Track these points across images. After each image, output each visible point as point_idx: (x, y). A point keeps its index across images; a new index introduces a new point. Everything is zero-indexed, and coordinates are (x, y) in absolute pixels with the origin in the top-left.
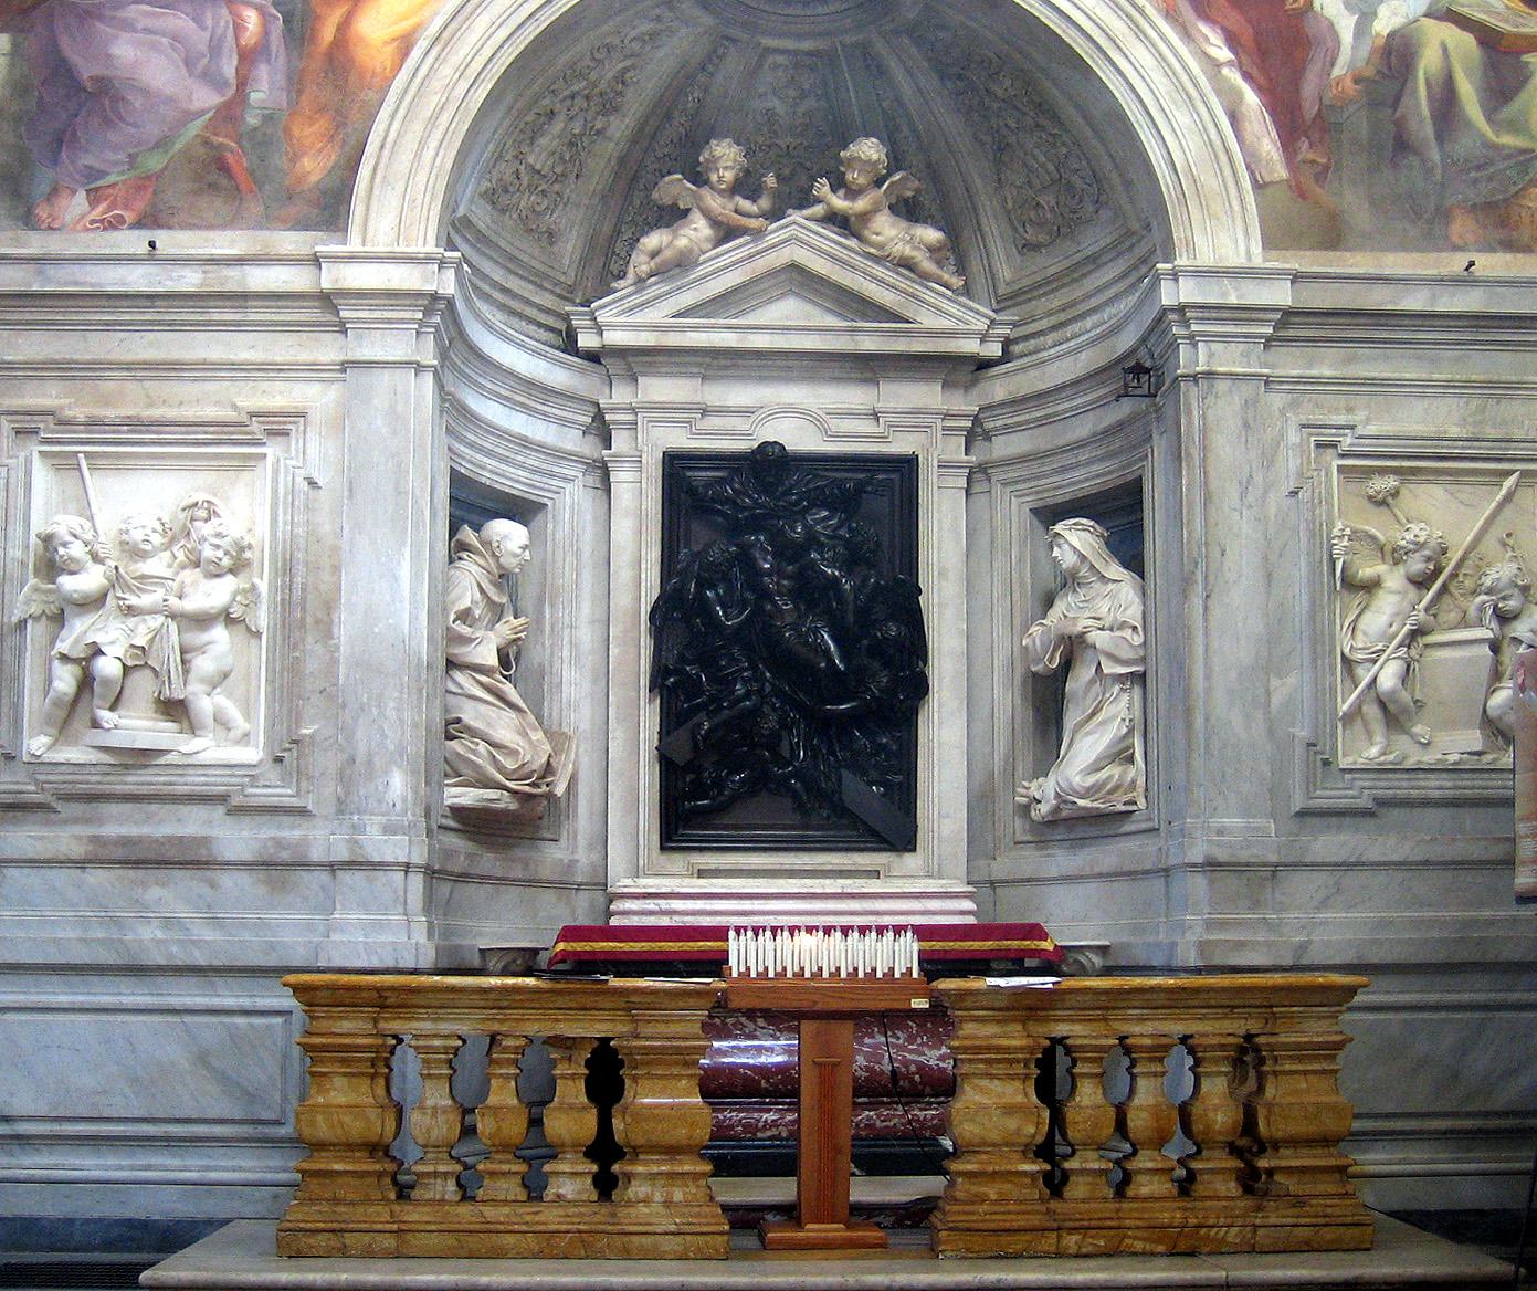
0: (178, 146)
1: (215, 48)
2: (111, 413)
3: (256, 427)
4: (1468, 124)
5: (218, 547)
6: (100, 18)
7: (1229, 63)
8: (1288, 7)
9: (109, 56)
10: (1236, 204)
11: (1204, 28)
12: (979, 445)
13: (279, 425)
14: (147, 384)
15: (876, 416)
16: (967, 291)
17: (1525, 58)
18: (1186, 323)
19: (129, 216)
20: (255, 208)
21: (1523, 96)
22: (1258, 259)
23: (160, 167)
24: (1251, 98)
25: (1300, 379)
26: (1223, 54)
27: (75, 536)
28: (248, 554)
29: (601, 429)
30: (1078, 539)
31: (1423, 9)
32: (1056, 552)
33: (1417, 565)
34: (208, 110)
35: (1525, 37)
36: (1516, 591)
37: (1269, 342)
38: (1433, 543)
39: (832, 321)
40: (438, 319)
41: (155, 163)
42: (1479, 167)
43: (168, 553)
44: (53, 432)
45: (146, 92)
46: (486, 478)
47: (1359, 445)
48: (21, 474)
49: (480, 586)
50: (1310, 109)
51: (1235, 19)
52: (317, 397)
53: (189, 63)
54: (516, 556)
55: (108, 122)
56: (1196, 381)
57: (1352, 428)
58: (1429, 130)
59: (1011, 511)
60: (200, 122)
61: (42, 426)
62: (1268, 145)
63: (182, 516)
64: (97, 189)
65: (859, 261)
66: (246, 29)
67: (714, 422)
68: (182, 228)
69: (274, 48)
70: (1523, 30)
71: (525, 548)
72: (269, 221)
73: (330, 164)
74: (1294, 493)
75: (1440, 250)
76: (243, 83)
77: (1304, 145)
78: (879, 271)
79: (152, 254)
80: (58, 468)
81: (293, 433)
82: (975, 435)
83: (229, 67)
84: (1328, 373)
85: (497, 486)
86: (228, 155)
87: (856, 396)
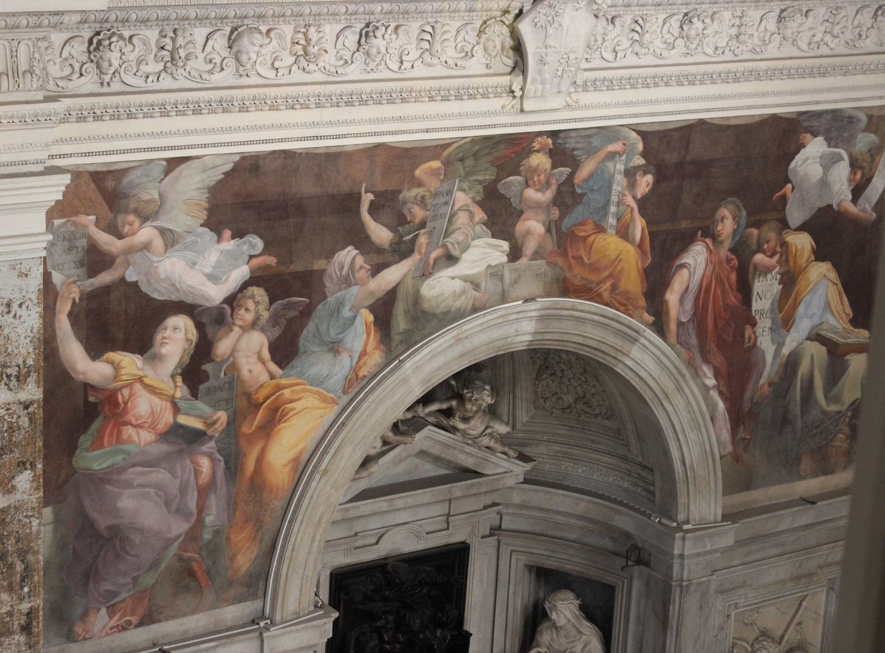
0: (164, 565)
4: (816, 402)
6: (109, 482)
8: (746, 346)
9: (117, 510)
11: (705, 368)
19: (135, 620)
20: (209, 596)
23: (153, 581)
26: (711, 382)
41: (149, 580)
42: (817, 427)
45: (142, 531)
50: (747, 406)
51: (719, 360)
53: (167, 504)
55: (118, 556)
60: (176, 545)
64: (113, 605)
66: (202, 472)
68: (167, 620)
69: (219, 485)
73: (253, 557)
75: (794, 481)
77: (741, 428)
86: (194, 564)
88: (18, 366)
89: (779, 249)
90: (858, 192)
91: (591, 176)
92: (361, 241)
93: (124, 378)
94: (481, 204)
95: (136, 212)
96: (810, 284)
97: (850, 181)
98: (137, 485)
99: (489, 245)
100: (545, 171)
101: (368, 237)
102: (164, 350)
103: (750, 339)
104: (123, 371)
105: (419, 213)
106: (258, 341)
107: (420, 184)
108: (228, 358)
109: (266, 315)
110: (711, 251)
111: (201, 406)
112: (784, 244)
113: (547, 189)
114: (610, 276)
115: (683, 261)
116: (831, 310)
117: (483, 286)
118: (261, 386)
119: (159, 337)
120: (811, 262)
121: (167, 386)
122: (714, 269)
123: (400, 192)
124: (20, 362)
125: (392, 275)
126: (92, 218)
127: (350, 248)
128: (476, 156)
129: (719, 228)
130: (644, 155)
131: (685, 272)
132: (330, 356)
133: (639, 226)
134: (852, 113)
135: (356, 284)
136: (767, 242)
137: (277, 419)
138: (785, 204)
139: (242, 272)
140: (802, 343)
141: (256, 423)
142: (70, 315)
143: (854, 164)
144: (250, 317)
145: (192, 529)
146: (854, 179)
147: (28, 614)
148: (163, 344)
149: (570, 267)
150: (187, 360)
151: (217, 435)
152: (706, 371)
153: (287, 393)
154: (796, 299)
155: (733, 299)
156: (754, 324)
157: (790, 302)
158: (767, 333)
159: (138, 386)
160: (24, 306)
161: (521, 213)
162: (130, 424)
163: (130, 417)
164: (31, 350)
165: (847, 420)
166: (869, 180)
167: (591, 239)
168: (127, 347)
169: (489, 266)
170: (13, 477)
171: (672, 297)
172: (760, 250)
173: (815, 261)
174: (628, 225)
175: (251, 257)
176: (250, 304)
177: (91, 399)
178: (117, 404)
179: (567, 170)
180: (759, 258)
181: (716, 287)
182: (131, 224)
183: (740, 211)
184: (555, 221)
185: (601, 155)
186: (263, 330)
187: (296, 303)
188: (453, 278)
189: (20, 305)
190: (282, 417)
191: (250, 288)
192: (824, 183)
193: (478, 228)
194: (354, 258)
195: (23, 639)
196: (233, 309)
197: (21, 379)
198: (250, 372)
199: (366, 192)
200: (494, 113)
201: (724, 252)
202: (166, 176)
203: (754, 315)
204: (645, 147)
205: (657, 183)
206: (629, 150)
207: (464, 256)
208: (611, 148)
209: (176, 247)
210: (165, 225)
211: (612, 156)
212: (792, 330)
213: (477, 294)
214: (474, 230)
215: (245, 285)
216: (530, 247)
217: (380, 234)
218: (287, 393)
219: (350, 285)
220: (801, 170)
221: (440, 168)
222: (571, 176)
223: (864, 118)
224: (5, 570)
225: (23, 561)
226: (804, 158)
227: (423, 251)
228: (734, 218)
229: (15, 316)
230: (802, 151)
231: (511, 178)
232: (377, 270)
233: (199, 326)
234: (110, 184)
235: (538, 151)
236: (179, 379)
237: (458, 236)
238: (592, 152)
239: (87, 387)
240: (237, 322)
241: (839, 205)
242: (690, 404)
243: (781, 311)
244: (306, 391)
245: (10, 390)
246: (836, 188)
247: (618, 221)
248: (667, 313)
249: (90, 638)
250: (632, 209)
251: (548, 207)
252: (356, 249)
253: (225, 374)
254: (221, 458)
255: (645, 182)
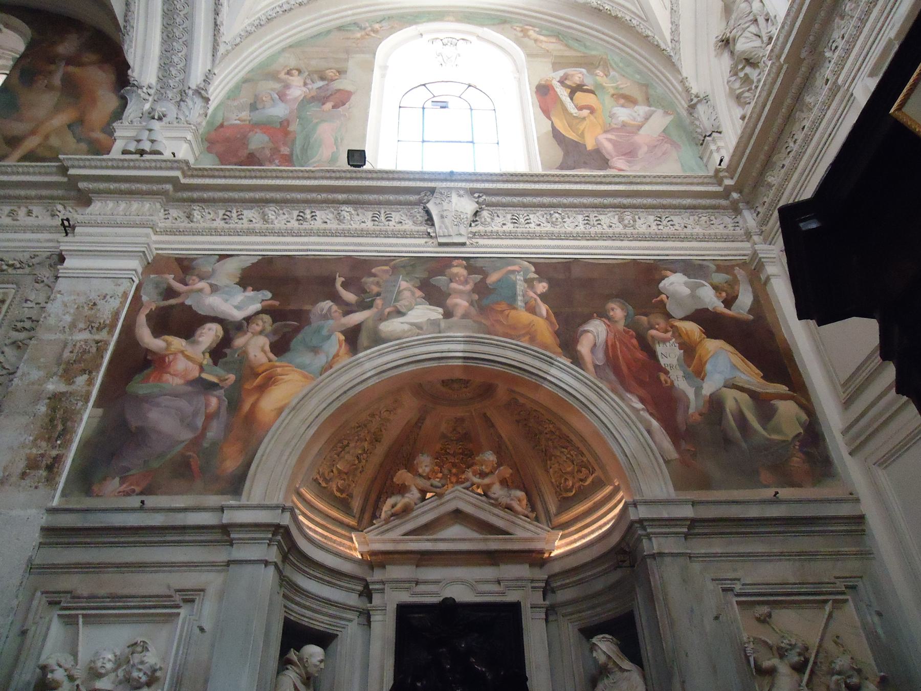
1: (195, 414)
2: (102, 592)
3: (178, 598)
4: (756, 431)
5: (140, 670)
7: (643, 409)
10: (658, 471)
12: (550, 595)
13: (190, 597)
14: (126, 575)
15: (499, 582)
16: (537, 519)
17: (772, 402)
18: (644, 529)
19: (138, 489)
21: (776, 416)
22: (672, 494)
24: (655, 423)
25: (707, 555)
26: (639, 406)
27: (60, 666)
28: (158, 674)
29: (367, 593)
30: (605, 646)
31: (722, 384)
32: (594, 655)
33: (795, 658)
34: (185, 441)
35: (771, 394)
36: (855, 673)
37: (686, 536)
38: (800, 645)
39: (476, 535)
40: (279, 538)
41: (155, 465)
43: (115, 674)
44: (70, 602)
46: (305, 622)
47: (744, 589)
48: (44, 629)
49: (295, 685)
51: (642, 392)
52: (212, 580)
53: (182, 420)
54: (316, 666)
56: (655, 559)
57: (739, 580)
58: (738, 434)
59: (569, 630)
60: (183, 445)
61: (62, 599)
62: (667, 444)
63: (127, 650)
64: (125, 477)
65: (487, 506)
67: (422, 588)
70: (767, 391)
71: (321, 661)
72: (206, 491)
74: (717, 618)
76: (205, 428)
78: (496, 511)
79: (142, 508)
80: (67, 624)
81: (197, 601)
82: (547, 590)
83: (200, 422)
84: (719, 550)
85: (312, 626)
87: (489, 572)
88: (100, 323)
89: (670, 329)
90: (729, 302)
91: (499, 280)
92: (335, 298)
93: (173, 350)
94: (420, 288)
95: (198, 276)
96: (710, 352)
97: (718, 297)
98: (165, 406)
99: (428, 309)
100: (463, 275)
101: (340, 297)
102: (200, 339)
103: (666, 382)
104: (172, 347)
105: (375, 289)
106: (263, 342)
107: (374, 275)
108: (242, 347)
109: (269, 328)
110: (609, 326)
111: (218, 370)
112: (672, 326)
113: (467, 284)
114: (528, 333)
115: (586, 329)
116: (739, 369)
117: (425, 328)
118: (262, 365)
119: (198, 332)
120: (704, 338)
121: (199, 356)
122: (615, 336)
123: (362, 278)
124: (102, 321)
125: (357, 318)
126: (173, 276)
127: (327, 301)
128: (413, 266)
129: (611, 313)
130: (536, 272)
131: (590, 334)
132: (312, 354)
133: (543, 309)
134: (700, 262)
135: (332, 319)
136: (658, 325)
137: (270, 383)
138: (665, 305)
139: (257, 306)
140: (720, 389)
141: (255, 384)
142: (147, 316)
143: (716, 288)
144: (258, 328)
145: (196, 438)
146: (721, 296)
147: (54, 458)
148: (200, 336)
149: (493, 325)
150: (214, 345)
151: (226, 387)
152: (631, 398)
153: (279, 370)
154: (700, 359)
155: (640, 355)
156: (667, 373)
157: (695, 361)
158: (680, 379)
159: (180, 356)
160: (113, 298)
161: (450, 295)
162: (169, 373)
163: (171, 370)
164: (110, 317)
165: (797, 447)
166: (736, 297)
167: (506, 312)
168: (178, 334)
169: (429, 320)
170: (76, 377)
171: (584, 348)
172: (652, 327)
173: (708, 337)
174: (534, 308)
175: (263, 300)
176: (260, 323)
177: (149, 357)
178: (164, 361)
179: (478, 277)
180: (653, 332)
181: (620, 347)
182: (193, 280)
183: (626, 306)
184: (476, 301)
185: (504, 271)
186: (266, 336)
187: (290, 325)
188: (402, 323)
189: (111, 297)
190: (274, 383)
191: (261, 315)
192: (693, 296)
193: (418, 299)
194: (330, 308)
195: (45, 474)
196: (248, 324)
197: (99, 329)
198: (255, 356)
199: (339, 277)
200: (419, 246)
201: (621, 326)
202: (218, 262)
203: (664, 366)
204: (535, 267)
205: (550, 287)
206: (526, 271)
207: (410, 312)
208: (510, 268)
209: (218, 292)
210: (213, 282)
211: (513, 272)
212: (705, 380)
213: (420, 332)
214: (416, 300)
215: (258, 313)
216: (459, 312)
217: (350, 297)
218: (279, 370)
219: (328, 319)
220: (671, 288)
221: (387, 270)
222: (483, 281)
223: (713, 267)
224: (50, 428)
225: (63, 425)
226: (670, 282)
227: (380, 307)
228: (622, 309)
229: (106, 301)
230: (666, 279)
231: (440, 277)
232: (346, 313)
233: (226, 330)
234: (186, 263)
235: (456, 266)
236: (207, 355)
237: (403, 302)
238: (496, 269)
239: (148, 351)
240: (249, 330)
241: (714, 309)
242: (615, 408)
243: (689, 366)
244: (293, 370)
245: (91, 333)
246: (707, 300)
247: (526, 304)
248: (582, 358)
249: (101, 496)
250: (535, 300)
251: (470, 292)
252: (332, 302)
253: (238, 356)
254: (226, 399)
255: (542, 287)
